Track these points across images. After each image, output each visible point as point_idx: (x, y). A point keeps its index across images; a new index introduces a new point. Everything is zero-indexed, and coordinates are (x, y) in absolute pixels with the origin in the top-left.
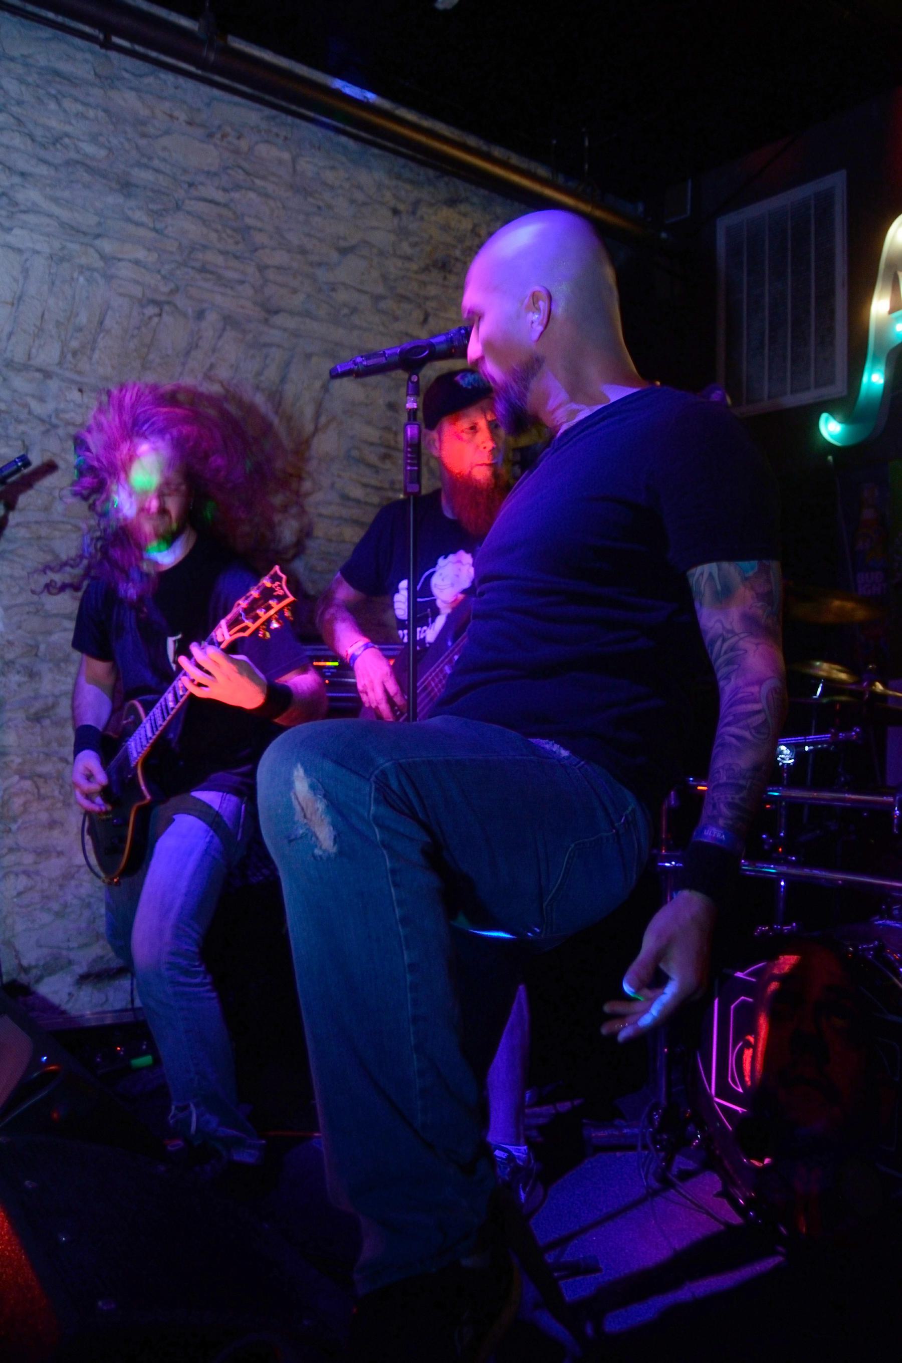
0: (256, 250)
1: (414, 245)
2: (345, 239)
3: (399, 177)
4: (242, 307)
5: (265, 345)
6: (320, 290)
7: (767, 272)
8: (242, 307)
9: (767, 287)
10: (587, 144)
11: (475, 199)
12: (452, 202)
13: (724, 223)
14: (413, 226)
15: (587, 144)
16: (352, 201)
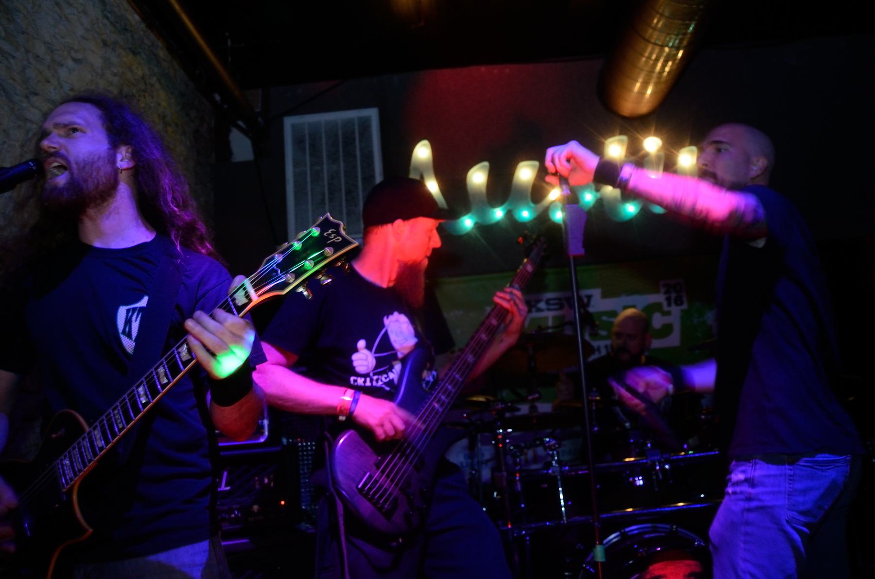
0: (23, 33)
1: (115, 75)
2: (76, 51)
3: (107, 18)
4: (14, 80)
5: (26, 120)
6: (62, 88)
7: (325, 156)
8: (14, 80)
9: (325, 167)
10: (229, 43)
11: (144, 56)
12: (135, 53)
13: (289, 122)
14: (115, 60)
15: (229, 43)
16: (82, 24)
